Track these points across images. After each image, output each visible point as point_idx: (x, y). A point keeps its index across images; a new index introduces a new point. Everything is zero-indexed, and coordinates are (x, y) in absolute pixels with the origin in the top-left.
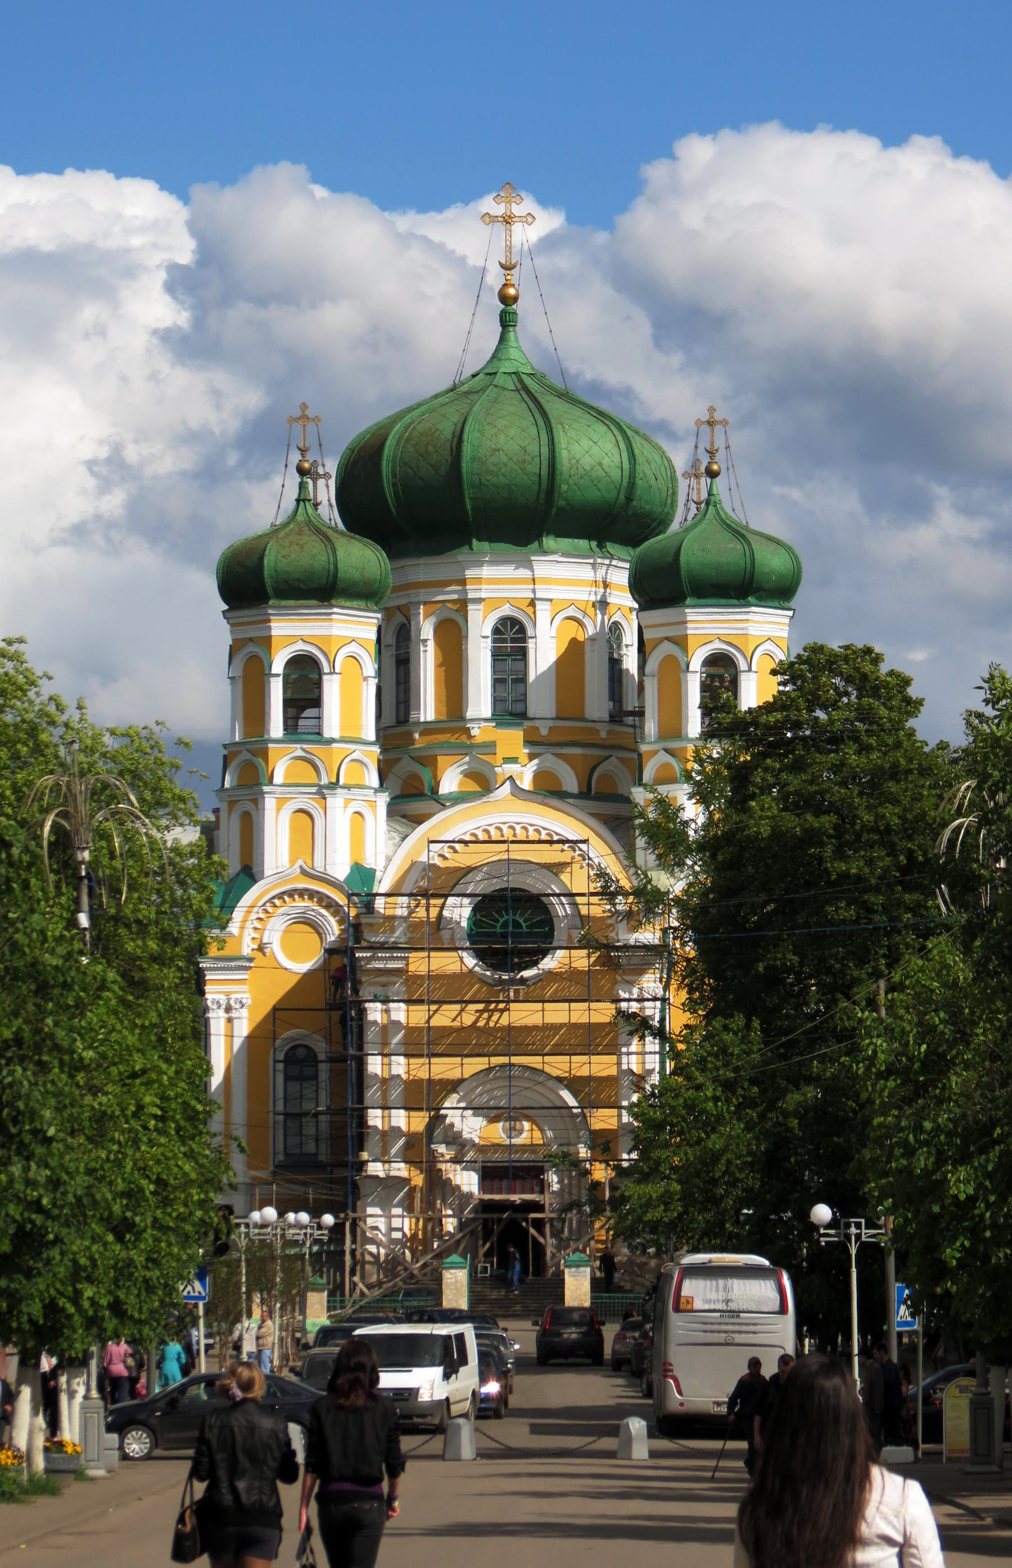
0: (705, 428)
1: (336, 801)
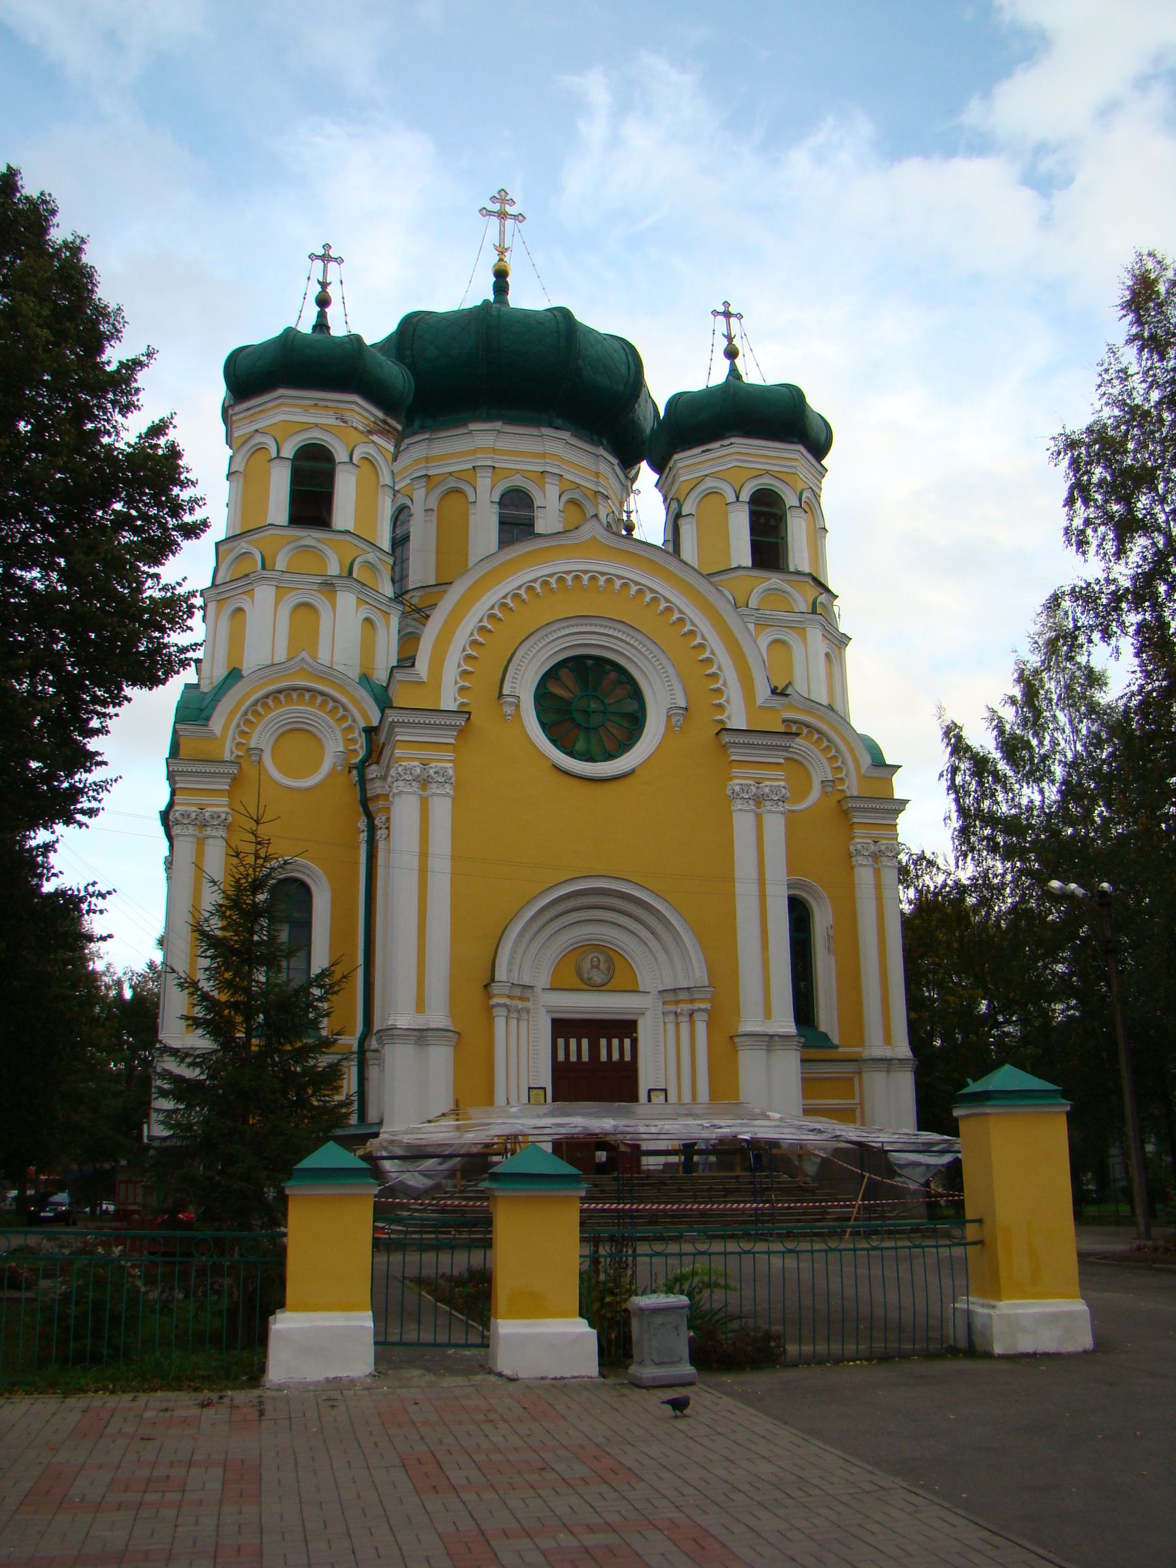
0: (721, 319)
1: (346, 600)
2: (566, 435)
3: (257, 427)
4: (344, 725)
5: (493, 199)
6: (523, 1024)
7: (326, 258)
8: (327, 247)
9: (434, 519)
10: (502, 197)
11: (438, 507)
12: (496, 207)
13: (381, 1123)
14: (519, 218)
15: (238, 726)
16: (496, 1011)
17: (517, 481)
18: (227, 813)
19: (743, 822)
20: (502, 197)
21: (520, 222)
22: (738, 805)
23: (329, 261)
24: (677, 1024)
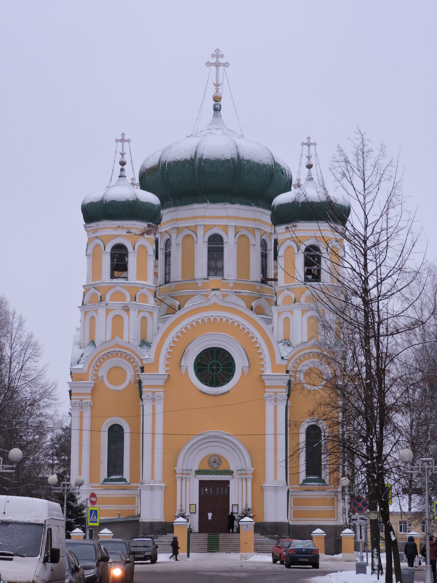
0: (306, 147)
2: (237, 206)
3: (97, 235)
4: (134, 365)
5: (213, 56)
6: (188, 483)
7: (123, 140)
8: (123, 134)
9: (180, 248)
10: (217, 54)
11: (182, 242)
12: (214, 60)
13: (139, 516)
14: (226, 65)
15: (94, 367)
16: (177, 479)
17: (216, 231)
18: (91, 402)
19: (269, 408)
20: (217, 54)
21: (227, 67)
22: (267, 402)
23: (124, 142)
24: (242, 482)
